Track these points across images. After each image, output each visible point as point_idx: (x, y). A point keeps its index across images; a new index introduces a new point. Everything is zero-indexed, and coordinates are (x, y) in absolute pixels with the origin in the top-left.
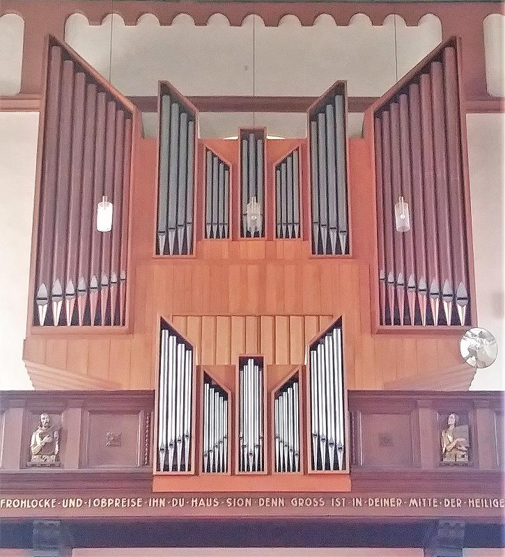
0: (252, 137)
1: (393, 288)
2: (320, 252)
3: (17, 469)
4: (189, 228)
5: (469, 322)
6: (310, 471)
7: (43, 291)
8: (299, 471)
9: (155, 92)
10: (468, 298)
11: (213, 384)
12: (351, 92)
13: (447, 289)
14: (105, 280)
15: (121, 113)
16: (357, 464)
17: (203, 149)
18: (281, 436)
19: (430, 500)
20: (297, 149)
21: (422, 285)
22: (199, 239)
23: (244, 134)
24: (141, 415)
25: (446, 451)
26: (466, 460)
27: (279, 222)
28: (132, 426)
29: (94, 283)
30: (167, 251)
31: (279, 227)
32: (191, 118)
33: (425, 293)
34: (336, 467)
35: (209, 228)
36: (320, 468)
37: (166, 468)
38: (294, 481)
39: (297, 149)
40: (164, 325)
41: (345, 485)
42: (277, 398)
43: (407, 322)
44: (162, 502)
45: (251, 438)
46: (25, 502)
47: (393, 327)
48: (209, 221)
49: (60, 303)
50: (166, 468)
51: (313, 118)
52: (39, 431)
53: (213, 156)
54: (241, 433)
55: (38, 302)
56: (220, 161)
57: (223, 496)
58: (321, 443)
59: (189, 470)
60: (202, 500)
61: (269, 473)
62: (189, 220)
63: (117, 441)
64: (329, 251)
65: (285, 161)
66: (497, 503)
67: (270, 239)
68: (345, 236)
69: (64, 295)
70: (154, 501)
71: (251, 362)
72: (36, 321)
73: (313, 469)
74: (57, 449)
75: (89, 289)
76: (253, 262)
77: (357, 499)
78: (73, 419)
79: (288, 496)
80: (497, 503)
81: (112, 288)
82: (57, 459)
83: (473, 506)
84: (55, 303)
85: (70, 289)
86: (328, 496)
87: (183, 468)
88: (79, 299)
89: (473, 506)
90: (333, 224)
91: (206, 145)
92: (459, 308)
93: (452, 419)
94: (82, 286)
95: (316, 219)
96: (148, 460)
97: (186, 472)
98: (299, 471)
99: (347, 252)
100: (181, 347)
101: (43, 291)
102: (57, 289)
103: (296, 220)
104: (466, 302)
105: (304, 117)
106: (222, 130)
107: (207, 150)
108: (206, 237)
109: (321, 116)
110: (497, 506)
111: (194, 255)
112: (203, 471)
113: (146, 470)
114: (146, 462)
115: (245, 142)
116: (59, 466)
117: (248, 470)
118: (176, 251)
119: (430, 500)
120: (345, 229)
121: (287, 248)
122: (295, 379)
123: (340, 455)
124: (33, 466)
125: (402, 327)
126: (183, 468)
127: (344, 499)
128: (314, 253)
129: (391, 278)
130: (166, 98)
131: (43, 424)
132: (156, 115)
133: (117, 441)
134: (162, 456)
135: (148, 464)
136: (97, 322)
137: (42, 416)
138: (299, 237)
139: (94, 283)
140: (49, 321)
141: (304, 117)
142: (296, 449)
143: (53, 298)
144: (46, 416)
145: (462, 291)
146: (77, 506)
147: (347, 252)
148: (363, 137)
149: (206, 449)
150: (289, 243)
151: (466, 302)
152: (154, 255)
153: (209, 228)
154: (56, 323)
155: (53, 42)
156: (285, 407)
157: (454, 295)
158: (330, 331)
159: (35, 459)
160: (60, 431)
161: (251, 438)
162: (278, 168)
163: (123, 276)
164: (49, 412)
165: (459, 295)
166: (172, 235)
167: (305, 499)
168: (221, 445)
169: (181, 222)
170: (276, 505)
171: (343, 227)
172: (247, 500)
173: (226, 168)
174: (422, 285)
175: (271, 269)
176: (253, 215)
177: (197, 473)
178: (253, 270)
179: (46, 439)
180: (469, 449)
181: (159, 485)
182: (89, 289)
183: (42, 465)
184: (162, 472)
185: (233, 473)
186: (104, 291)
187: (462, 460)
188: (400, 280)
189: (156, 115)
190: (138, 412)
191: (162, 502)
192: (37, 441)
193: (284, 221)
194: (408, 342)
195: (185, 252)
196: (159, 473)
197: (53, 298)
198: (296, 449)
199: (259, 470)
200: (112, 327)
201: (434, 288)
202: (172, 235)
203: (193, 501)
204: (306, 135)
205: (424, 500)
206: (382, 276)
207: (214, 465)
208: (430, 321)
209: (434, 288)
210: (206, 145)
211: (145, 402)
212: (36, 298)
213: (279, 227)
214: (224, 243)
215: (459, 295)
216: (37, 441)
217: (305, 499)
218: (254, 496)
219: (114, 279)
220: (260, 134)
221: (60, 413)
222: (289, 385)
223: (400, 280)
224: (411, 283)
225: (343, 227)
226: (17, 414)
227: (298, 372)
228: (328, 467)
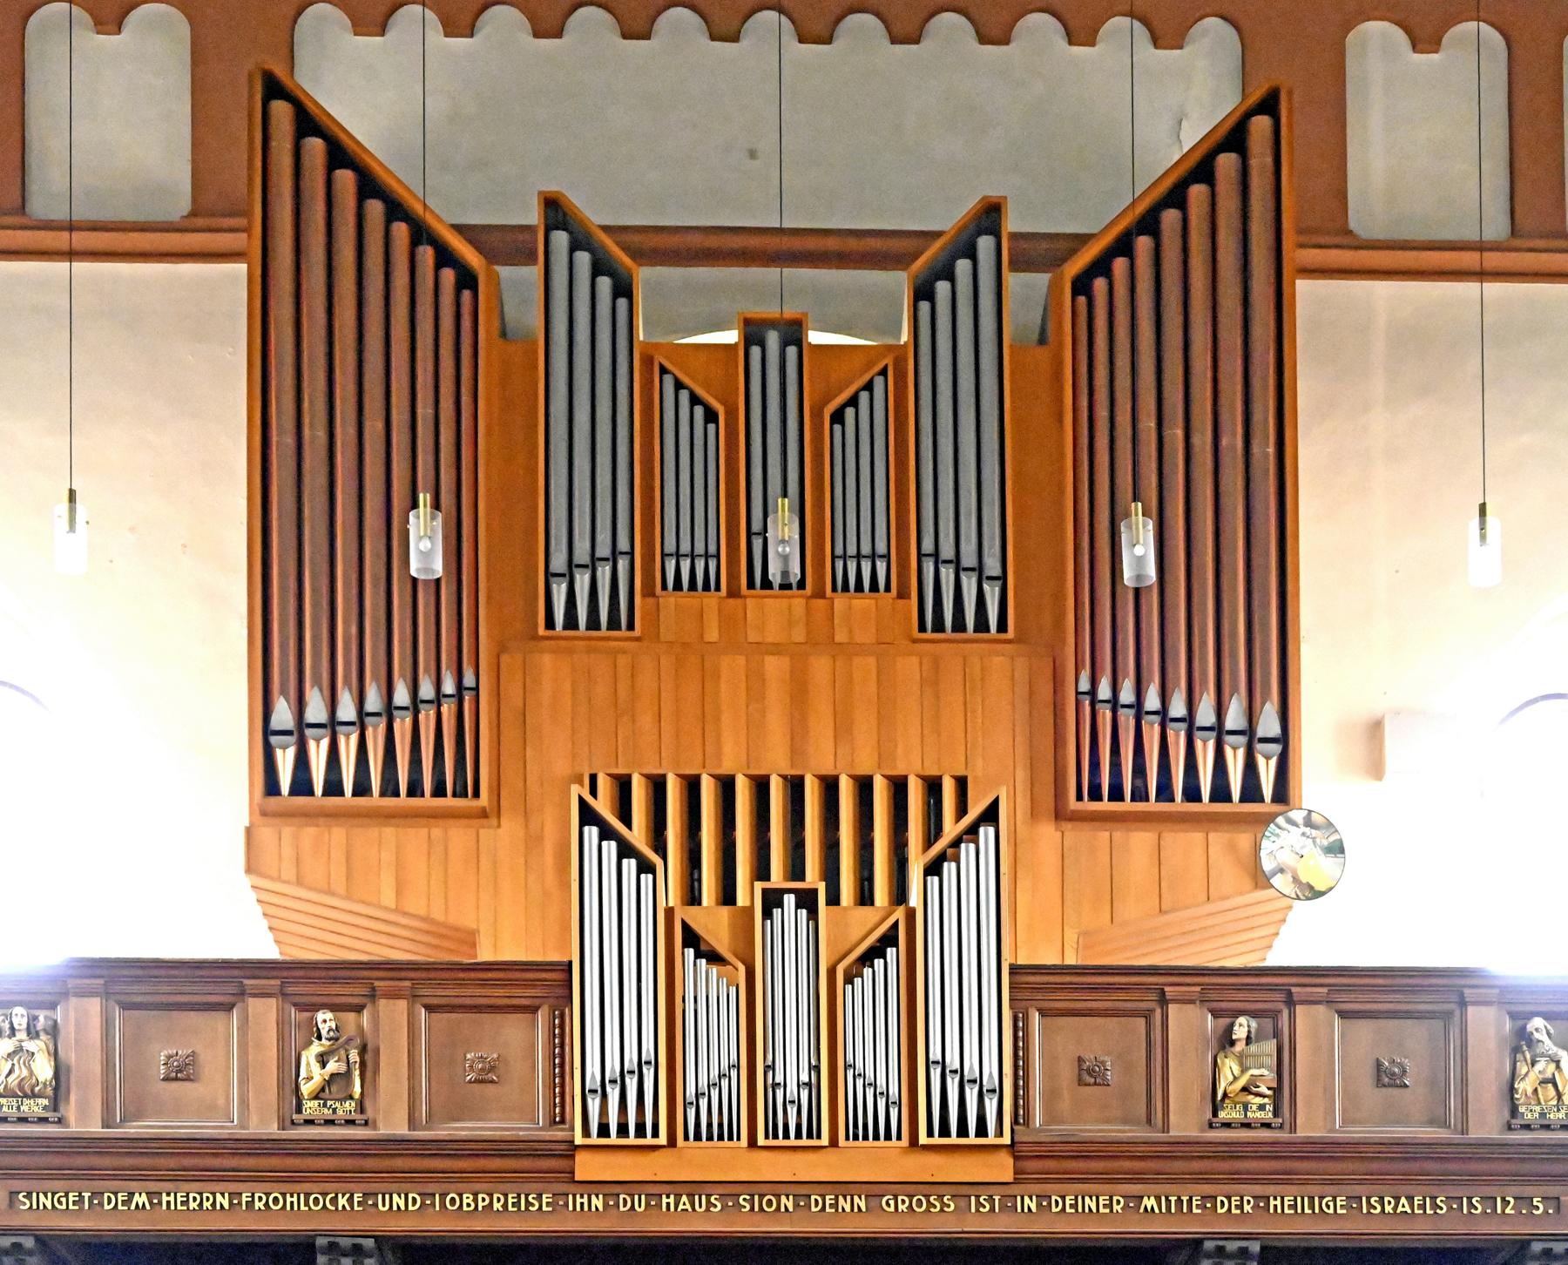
0: (773, 339)
1: (1108, 714)
2: (939, 626)
3: (272, 1129)
4: (622, 564)
5: (1282, 794)
6: (923, 1139)
7: (283, 715)
8: (899, 1138)
9: (533, 216)
10: (1284, 739)
11: (703, 947)
12: (1012, 223)
13: (1234, 718)
14: (426, 691)
15: (448, 275)
16: (1027, 1123)
17: (654, 366)
18: (859, 1064)
19: (1185, 1199)
20: (884, 372)
21: (1178, 708)
22: (649, 592)
23: (753, 333)
24: (542, 1017)
25: (1225, 1095)
26: (1267, 1115)
27: (839, 551)
28: (520, 1040)
29: (402, 696)
30: (570, 621)
31: (839, 564)
32: (623, 289)
33: (1183, 726)
34: (982, 1131)
35: (671, 565)
36: (945, 1132)
37: (604, 1131)
38: (883, 1161)
39: (884, 372)
40: (588, 816)
41: (1002, 1168)
42: (849, 980)
43: (1140, 795)
44: (598, 1202)
45: (793, 1071)
46: (295, 1199)
47: (1105, 805)
48: (670, 547)
49: (325, 743)
50: (604, 1131)
51: (923, 292)
52: (316, 1048)
53: (679, 385)
54: (770, 1057)
55: (274, 740)
56: (695, 400)
57: (731, 1190)
58: (949, 1080)
59: (655, 1134)
60: (684, 1198)
61: (834, 1143)
62: (623, 545)
63: (488, 1075)
64: (959, 625)
65: (853, 401)
67: (820, 594)
68: (997, 589)
69: (333, 725)
70: (579, 1200)
71: (789, 900)
72: (272, 788)
73: (930, 1134)
74: (357, 1090)
75: (390, 709)
76: (776, 649)
77: (1027, 1199)
78: (391, 1019)
79: (874, 1190)
81: (445, 709)
82: (361, 1108)
84: (312, 744)
85: (347, 711)
86: (963, 1190)
87: (641, 1131)
88: (369, 733)
90: (969, 559)
91: (660, 359)
92: (1261, 761)
94: (373, 702)
95: (928, 546)
96: (563, 1113)
97: (649, 1140)
98: (899, 1138)
99: (1002, 627)
100: (630, 865)
101: (283, 715)
102: (316, 710)
103: (881, 548)
104: (1276, 748)
105: (899, 282)
106: (698, 320)
107: (663, 370)
108: (664, 587)
109: (942, 287)
111: (637, 632)
112: (686, 1138)
113: (559, 1134)
114: (559, 1118)
115: (756, 351)
116: (366, 1123)
117: (786, 1136)
118: (593, 623)
119: (1185, 1199)
120: (997, 572)
121: (857, 614)
122: (890, 939)
123: (991, 1106)
124: (310, 1122)
125: (1127, 805)
126: (641, 1131)
127: (997, 1198)
128: (922, 628)
129: (1104, 692)
130: (561, 239)
131: (324, 1033)
132: (534, 272)
133: (488, 1075)
134: (594, 1105)
135: (563, 1121)
136: (415, 789)
137: (320, 1016)
138: (888, 589)
139: (402, 696)
140: (302, 785)
141: (899, 282)
142: (894, 1090)
143: (309, 732)
144: (329, 1015)
145: (1269, 724)
146: (411, 1208)
147: (1002, 627)
148: (1042, 340)
149: (691, 1090)
150: (863, 603)
151: (1276, 748)
152: (542, 631)
153: (671, 565)
154: (318, 788)
155: (274, 89)
156: (870, 1003)
157: (1249, 732)
158: (972, 831)
159: (311, 1107)
160: (363, 1050)
161: (793, 1071)
162: (838, 417)
163: (469, 681)
164: (333, 1008)
165: (1260, 733)
166: (582, 581)
167: (911, 1197)
168: (725, 1083)
169: (604, 550)
170: (848, 1209)
171: (992, 566)
172: (783, 1199)
173: (711, 416)
174: (1178, 708)
175: (820, 667)
176: (783, 541)
177: (672, 1142)
178: (775, 667)
179: (332, 1066)
180: (1277, 1091)
181: (587, 1167)
182: (390, 709)
183: (330, 1122)
184: (595, 1140)
185: (752, 1143)
186: (427, 717)
187: (1259, 1115)
188: (1127, 696)
189: (534, 272)
190: (533, 1010)
191: (598, 1202)
192: (313, 1074)
193: (852, 550)
194: (1140, 841)
195: (614, 624)
196: (588, 1141)
197: (309, 732)
198: (894, 1090)
199: (810, 1136)
200: (449, 801)
201: (1205, 714)
202: (582, 581)
203: (665, 1200)
204: (905, 337)
205: (1173, 1199)
206: (1084, 685)
207: (710, 1125)
208: (1192, 794)
209: (1205, 714)
210: (660, 359)
211: (550, 987)
212: (267, 732)
213: (839, 564)
214: (711, 601)
215: (1260, 733)
216: (313, 1074)
217: (911, 1197)
218: (801, 1189)
219: (449, 687)
220: (793, 334)
221: (359, 1009)
222: (876, 952)
223: (1127, 696)
224: (1152, 701)
225: (992, 566)
226: (264, 1012)
227: (896, 923)
228: (963, 1132)
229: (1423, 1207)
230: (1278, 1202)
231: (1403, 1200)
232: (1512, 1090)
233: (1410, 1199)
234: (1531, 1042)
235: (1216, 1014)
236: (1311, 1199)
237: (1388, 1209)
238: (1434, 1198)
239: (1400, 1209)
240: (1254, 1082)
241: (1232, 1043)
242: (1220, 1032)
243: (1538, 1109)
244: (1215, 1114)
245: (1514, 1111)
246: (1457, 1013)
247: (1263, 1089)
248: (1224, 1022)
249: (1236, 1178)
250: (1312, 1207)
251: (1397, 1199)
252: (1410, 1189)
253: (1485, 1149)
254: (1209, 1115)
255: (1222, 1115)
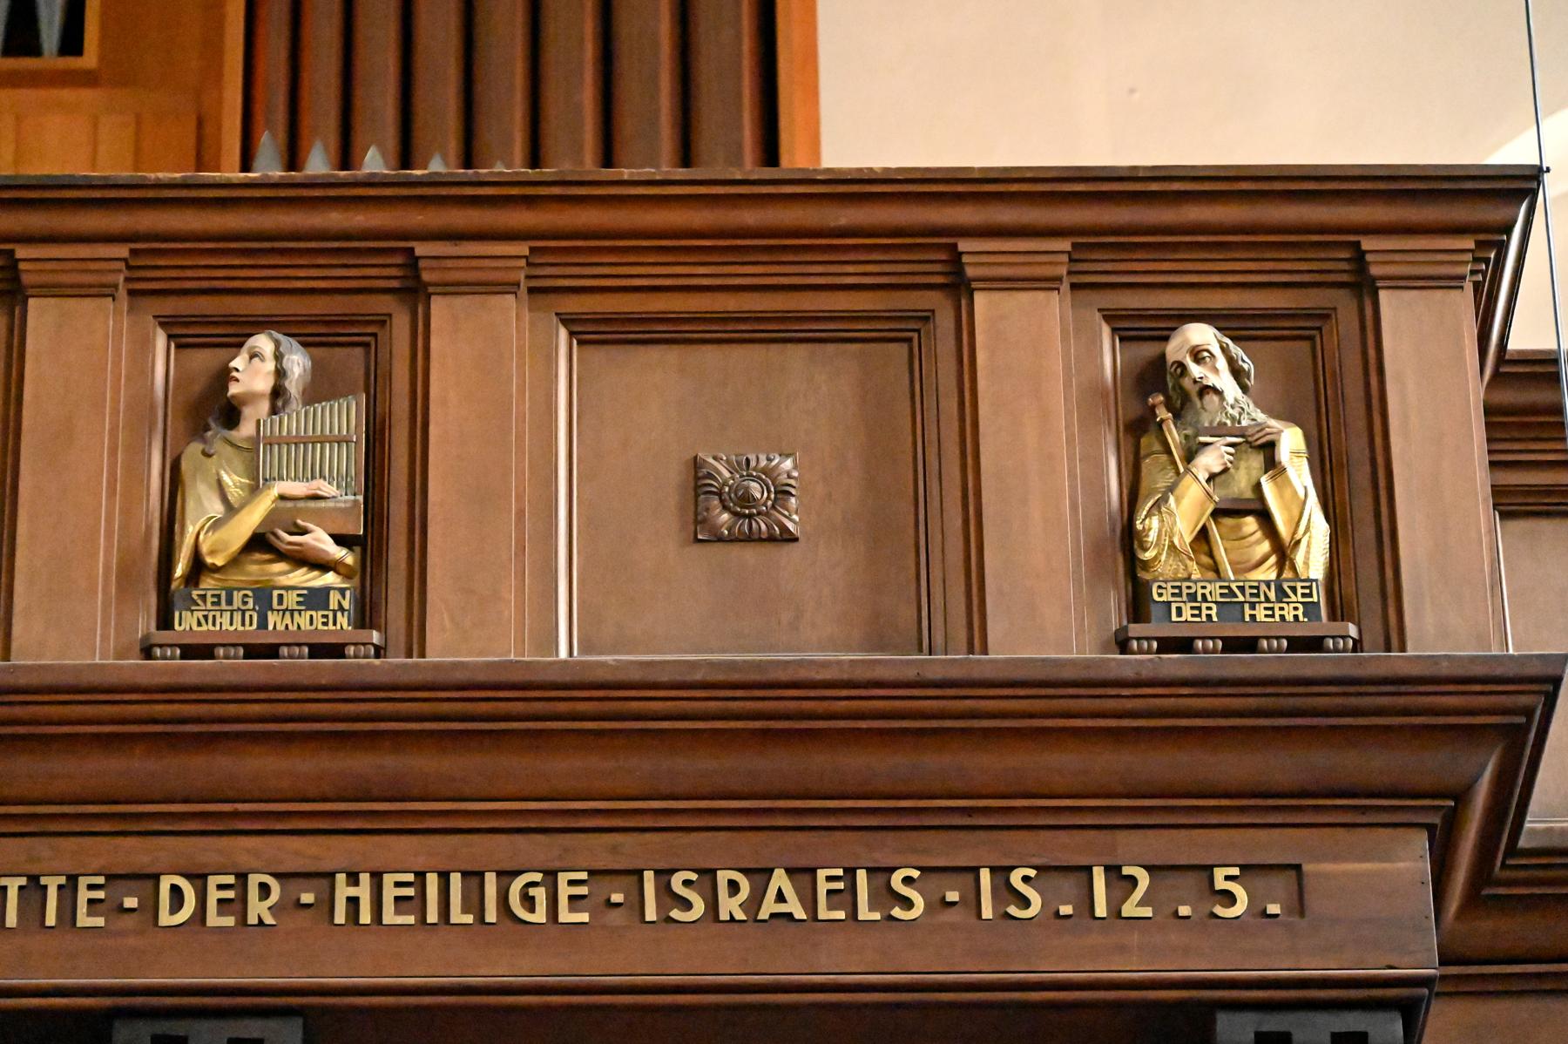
19: (52, 884)
25: (198, 567)
66: (540, 894)
80: (540, 894)
83: (365, 917)
89: (365, 917)
93: (252, 373)
110: (540, 916)
119: (52, 884)
180: (368, 542)
229: (845, 897)
230: (364, 891)
231: (780, 879)
232: (1130, 538)
233: (803, 874)
234: (1185, 399)
235: (183, 335)
236: (474, 877)
237: (730, 906)
238: (880, 873)
239: (769, 907)
240: (288, 515)
241: (231, 414)
242: (197, 388)
243: (1214, 590)
244: (165, 622)
245: (1138, 604)
246: (945, 321)
247: (320, 540)
248: (204, 360)
249: (222, 815)
250: (475, 903)
251: (760, 875)
252: (803, 847)
253: (1047, 706)
254: (145, 623)
255: (187, 623)
